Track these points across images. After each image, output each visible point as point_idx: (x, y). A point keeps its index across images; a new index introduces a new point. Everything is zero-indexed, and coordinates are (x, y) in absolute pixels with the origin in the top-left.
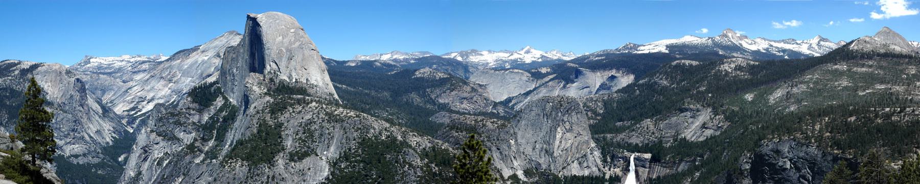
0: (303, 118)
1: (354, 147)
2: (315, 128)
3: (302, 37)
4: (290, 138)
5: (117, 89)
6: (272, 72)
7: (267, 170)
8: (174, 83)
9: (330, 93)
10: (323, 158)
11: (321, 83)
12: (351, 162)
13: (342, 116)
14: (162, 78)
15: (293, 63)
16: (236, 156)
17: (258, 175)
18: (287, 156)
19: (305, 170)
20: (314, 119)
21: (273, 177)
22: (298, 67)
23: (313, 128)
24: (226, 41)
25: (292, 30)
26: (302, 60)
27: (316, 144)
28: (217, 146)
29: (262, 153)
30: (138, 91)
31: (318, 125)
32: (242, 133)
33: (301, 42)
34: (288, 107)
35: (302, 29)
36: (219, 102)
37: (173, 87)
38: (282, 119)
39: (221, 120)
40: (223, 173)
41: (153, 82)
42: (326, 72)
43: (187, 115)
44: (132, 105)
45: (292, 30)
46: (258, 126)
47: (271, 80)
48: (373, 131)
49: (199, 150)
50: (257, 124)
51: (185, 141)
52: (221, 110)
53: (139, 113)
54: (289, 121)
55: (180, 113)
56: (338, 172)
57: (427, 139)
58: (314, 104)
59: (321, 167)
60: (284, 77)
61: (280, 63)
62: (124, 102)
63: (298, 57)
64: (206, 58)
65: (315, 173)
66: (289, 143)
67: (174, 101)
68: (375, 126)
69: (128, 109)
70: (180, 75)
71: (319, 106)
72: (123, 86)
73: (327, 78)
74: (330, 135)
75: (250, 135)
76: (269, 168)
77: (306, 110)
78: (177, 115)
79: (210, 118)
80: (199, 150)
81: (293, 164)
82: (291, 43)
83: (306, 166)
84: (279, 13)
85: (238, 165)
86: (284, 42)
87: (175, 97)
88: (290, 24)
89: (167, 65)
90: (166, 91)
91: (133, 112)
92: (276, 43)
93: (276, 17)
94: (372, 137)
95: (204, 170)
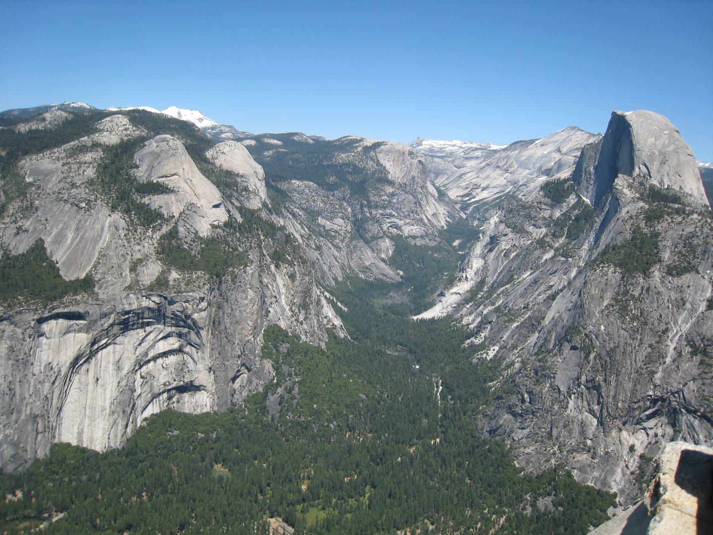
0: (683, 231)
2: (698, 243)
3: (678, 140)
4: (668, 251)
6: (642, 175)
7: (642, 280)
8: (511, 173)
9: (705, 205)
10: (706, 277)
14: (498, 167)
15: (666, 167)
16: (608, 261)
17: (632, 285)
18: (664, 269)
19: (684, 286)
20: (697, 232)
21: (648, 289)
22: (672, 173)
23: (695, 242)
24: (567, 136)
25: (666, 132)
26: (677, 166)
27: (699, 260)
28: (568, 244)
29: (637, 262)
31: (702, 240)
32: (613, 237)
34: (666, 216)
35: (678, 132)
36: (572, 200)
37: (508, 178)
38: (659, 228)
39: (573, 218)
40: (594, 277)
41: (489, 169)
42: (701, 181)
43: (538, 210)
44: (466, 191)
45: (666, 132)
46: (631, 232)
47: (641, 184)
49: (549, 245)
50: (630, 230)
51: (534, 235)
52: (574, 207)
53: (473, 200)
55: (531, 206)
58: (695, 216)
60: (655, 182)
61: (652, 166)
63: (673, 162)
64: (546, 152)
65: (696, 292)
66: (666, 255)
67: (510, 191)
69: (462, 194)
70: (517, 166)
71: (702, 219)
72: (457, 172)
73: (702, 189)
75: (621, 240)
76: (644, 279)
77: (687, 222)
78: (528, 208)
79: (562, 215)
80: (549, 245)
81: (670, 278)
84: (652, 113)
85: (610, 271)
87: (511, 187)
89: (504, 154)
90: (501, 181)
91: (467, 199)
92: (648, 144)
93: (648, 116)
95: (559, 267)
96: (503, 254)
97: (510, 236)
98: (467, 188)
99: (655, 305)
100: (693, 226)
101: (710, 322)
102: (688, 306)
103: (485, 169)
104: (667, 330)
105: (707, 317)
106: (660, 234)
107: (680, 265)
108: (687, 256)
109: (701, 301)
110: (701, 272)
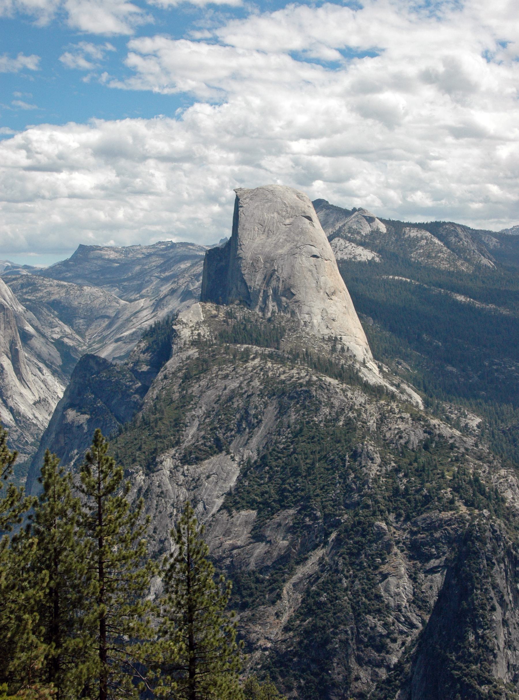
0: (225, 389)
1: (284, 440)
3: (303, 232)
4: (196, 423)
5: (113, 315)
10: (237, 458)
11: (319, 317)
12: (271, 468)
13: (288, 382)
15: (274, 283)
19: (203, 476)
20: (242, 389)
23: (235, 405)
27: (233, 433)
29: (140, 449)
30: (145, 318)
33: (295, 243)
45: (288, 221)
48: (327, 410)
54: (205, 392)
56: (246, 484)
57: (423, 426)
58: (257, 361)
59: (228, 474)
62: (117, 341)
63: (284, 274)
68: (336, 403)
69: (122, 354)
74: (257, 418)
76: (147, 475)
77: (237, 373)
82: (276, 246)
83: (205, 471)
86: (266, 244)
88: (289, 209)
93: (270, 196)
94: (320, 422)
96: (72, 463)
97: (86, 427)
98: (131, 341)
99: (151, 515)
100: (241, 378)
101: (218, 528)
102: (200, 506)
103: (165, 300)
104: (162, 551)
105: (217, 520)
106: (192, 397)
107: (204, 444)
108: (215, 428)
109: (218, 497)
110: (232, 451)
